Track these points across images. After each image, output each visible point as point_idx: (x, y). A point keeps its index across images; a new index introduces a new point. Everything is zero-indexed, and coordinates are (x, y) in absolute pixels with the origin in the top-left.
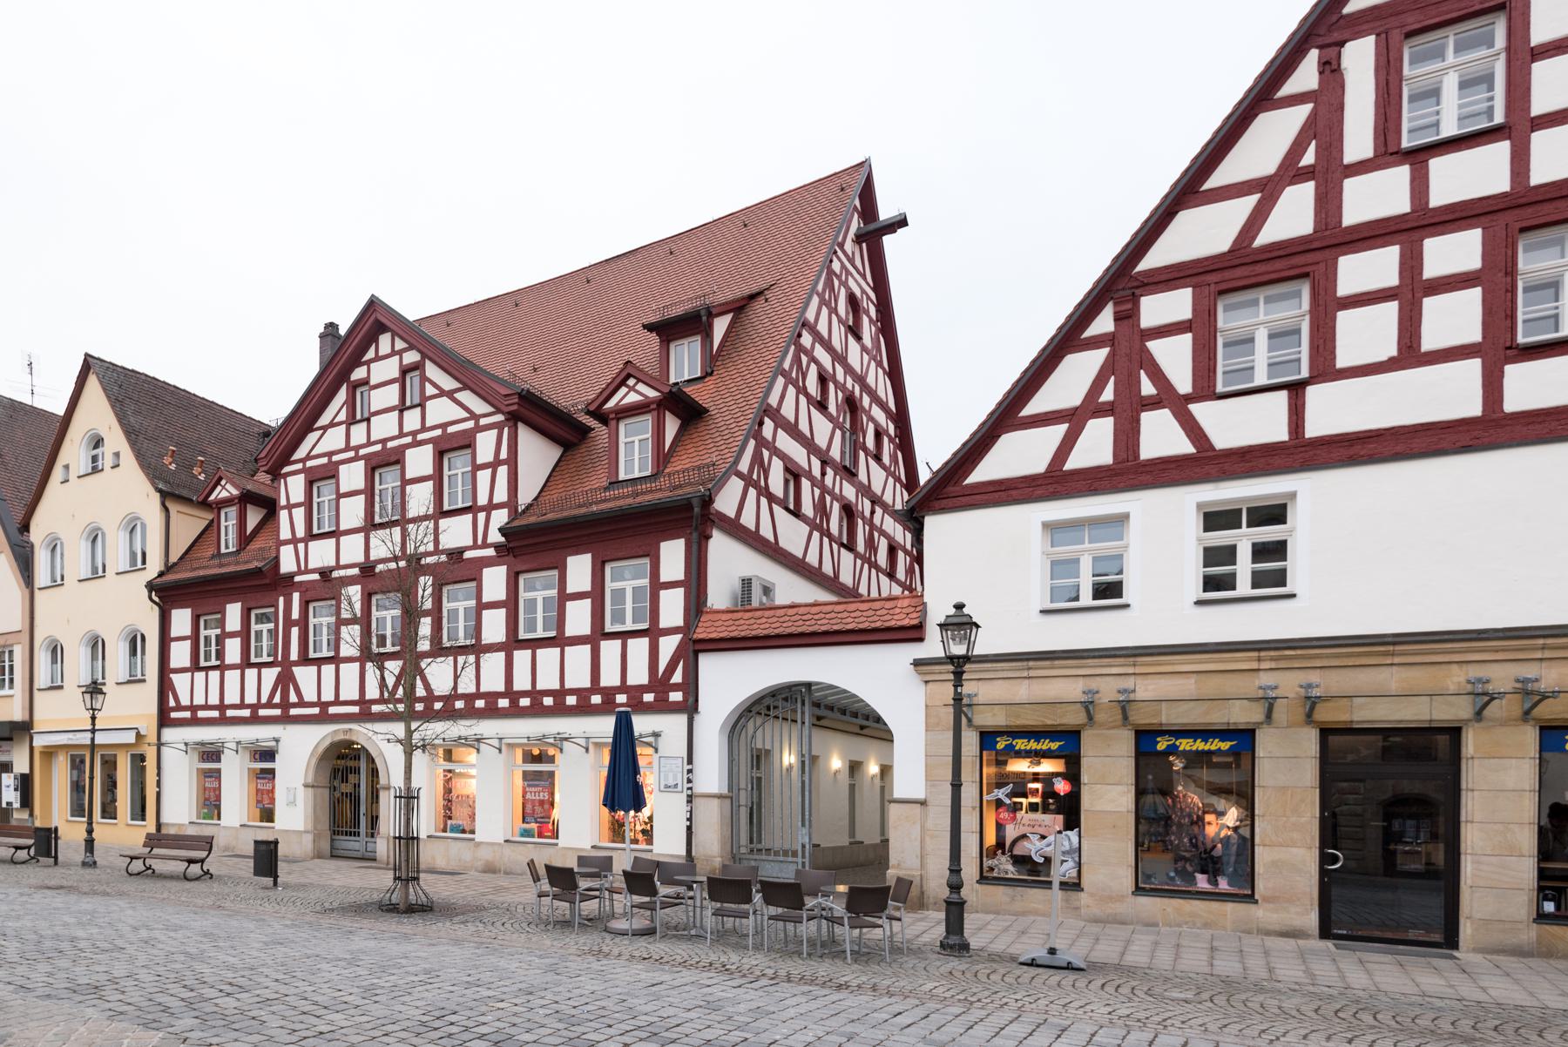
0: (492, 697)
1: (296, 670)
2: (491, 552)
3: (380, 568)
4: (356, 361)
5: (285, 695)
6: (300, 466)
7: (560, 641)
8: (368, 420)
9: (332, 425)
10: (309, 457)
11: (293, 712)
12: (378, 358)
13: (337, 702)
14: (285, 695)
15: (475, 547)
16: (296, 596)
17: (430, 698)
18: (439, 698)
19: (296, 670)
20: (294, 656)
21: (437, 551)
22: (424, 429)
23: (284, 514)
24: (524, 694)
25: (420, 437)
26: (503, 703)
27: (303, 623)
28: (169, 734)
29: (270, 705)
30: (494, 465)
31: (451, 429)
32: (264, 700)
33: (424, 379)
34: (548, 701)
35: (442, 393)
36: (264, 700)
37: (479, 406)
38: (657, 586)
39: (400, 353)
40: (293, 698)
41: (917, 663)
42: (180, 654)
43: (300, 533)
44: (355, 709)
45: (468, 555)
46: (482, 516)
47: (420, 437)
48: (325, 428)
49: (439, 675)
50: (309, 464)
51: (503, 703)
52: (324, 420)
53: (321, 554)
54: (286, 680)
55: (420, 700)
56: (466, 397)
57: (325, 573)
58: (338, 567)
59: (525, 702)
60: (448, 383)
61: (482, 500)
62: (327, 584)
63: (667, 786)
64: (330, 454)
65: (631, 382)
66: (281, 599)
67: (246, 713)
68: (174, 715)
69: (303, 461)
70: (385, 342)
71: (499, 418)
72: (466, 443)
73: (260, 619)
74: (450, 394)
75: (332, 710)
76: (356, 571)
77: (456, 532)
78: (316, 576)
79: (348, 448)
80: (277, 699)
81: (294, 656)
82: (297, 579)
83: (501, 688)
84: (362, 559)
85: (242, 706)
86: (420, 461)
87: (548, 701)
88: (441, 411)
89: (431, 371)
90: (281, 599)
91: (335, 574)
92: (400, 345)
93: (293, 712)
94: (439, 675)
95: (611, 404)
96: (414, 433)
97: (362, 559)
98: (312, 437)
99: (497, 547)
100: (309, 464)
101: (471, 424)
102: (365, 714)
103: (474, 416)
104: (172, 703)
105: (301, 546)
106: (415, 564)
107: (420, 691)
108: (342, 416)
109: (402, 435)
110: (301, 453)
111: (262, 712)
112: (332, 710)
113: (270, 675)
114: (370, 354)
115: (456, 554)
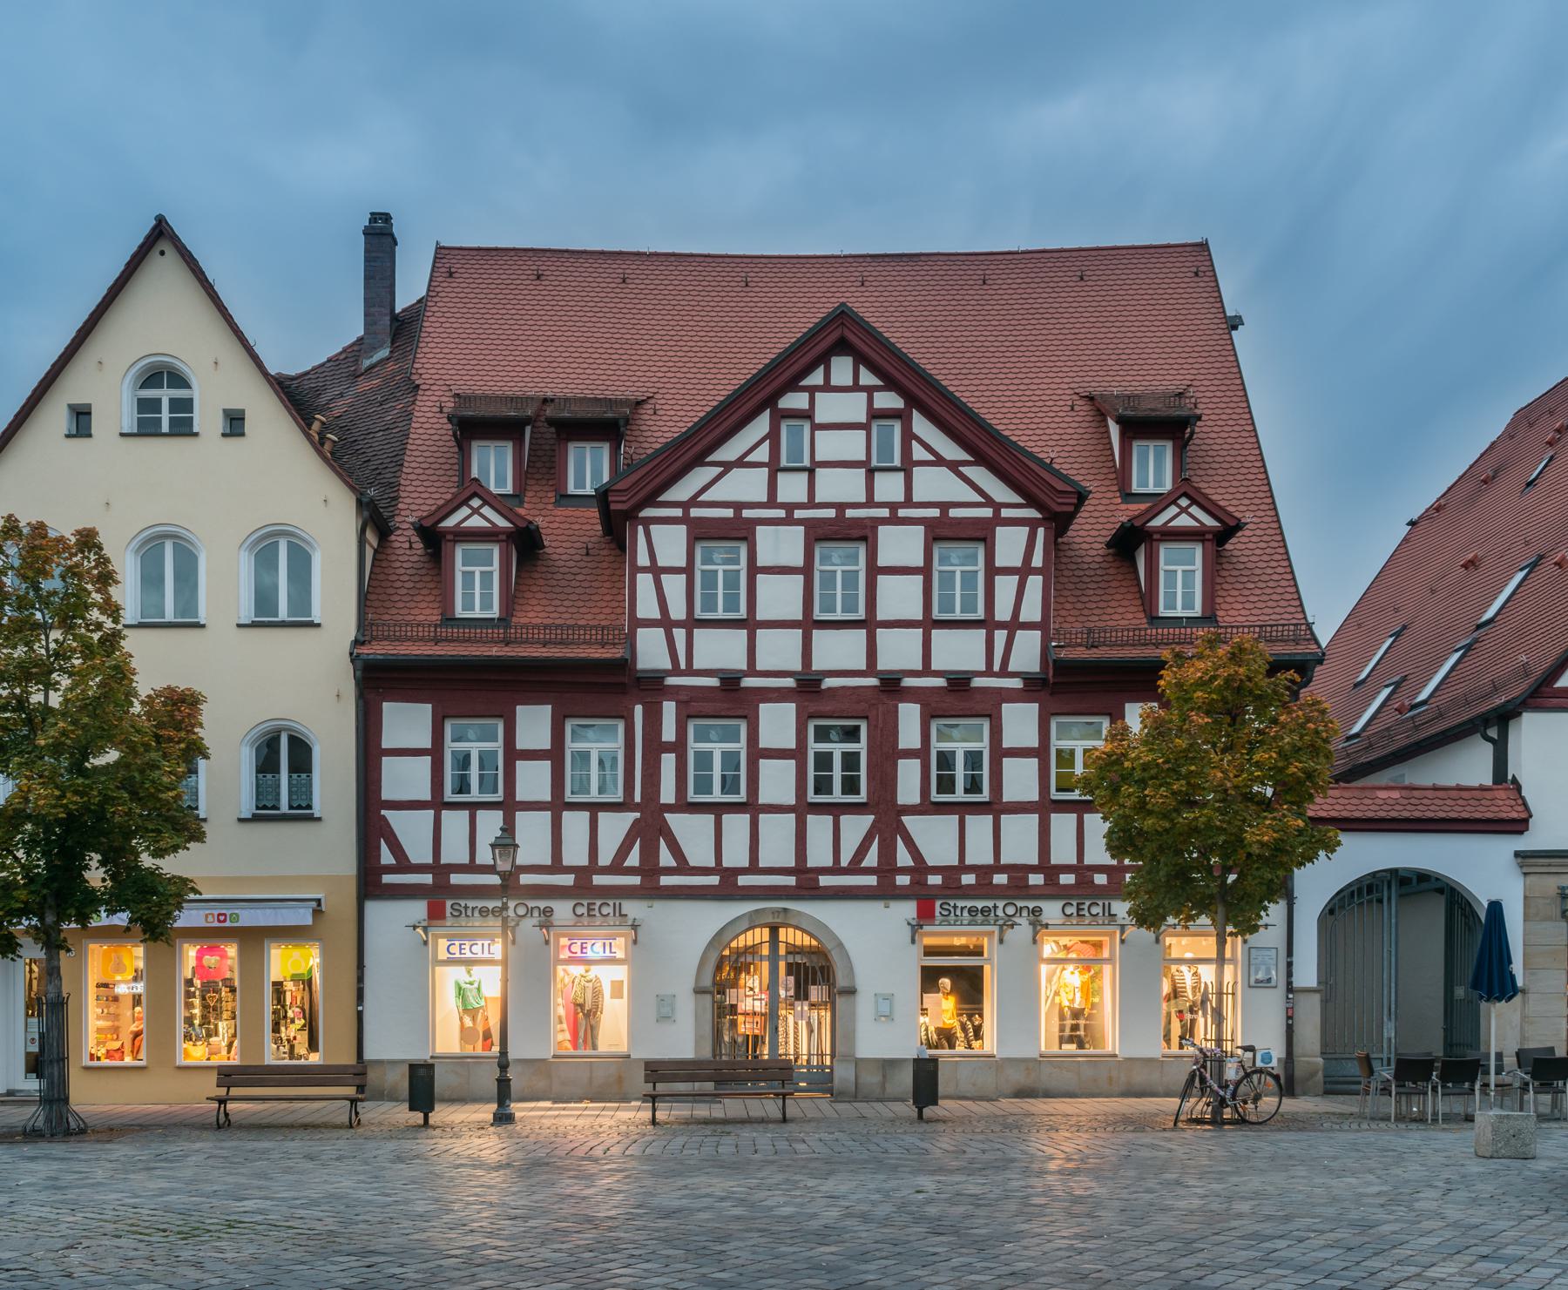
0: (1018, 872)
1: (670, 817)
2: (1016, 683)
3: (829, 682)
4: (793, 385)
5: (649, 853)
6: (678, 512)
7: (996, 808)
8: (811, 471)
9: (741, 463)
10: (693, 502)
11: (665, 880)
12: (827, 387)
13: (754, 868)
14: (649, 853)
15: (989, 672)
16: (669, 709)
17: (920, 868)
18: (936, 870)
19: (670, 817)
20: (668, 795)
21: (926, 671)
22: (909, 502)
23: (645, 582)
24: (1067, 869)
25: (798, 514)
26: (1036, 879)
27: (679, 747)
28: (373, 909)
29: (617, 867)
30: (1024, 571)
31: (953, 513)
32: (605, 859)
33: (908, 436)
34: (1101, 879)
35: (939, 461)
36: (605, 859)
37: (1000, 492)
38: (999, 753)
39: (870, 390)
40: (666, 858)
41: (1517, 854)
42: (405, 778)
43: (678, 611)
44: (791, 881)
45: (978, 682)
46: (1000, 636)
47: (902, 513)
48: (727, 466)
49: (935, 839)
50: (695, 512)
51: (1036, 879)
52: (730, 451)
53: (719, 651)
54: (651, 828)
55: (904, 871)
56: (979, 475)
57: (730, 681)
58: (752, 671)
59: (1067, 879)
60: (952, 451)
61: (1003, 612)
62: (733, 697)
63: (1257, 981)
64: (738, 506)
65: (476, 503)
66: (639, 709)
67: (568, 880)
68: (387, 879)
69: (686, 506)
70: (842, 369)
71: (1032, 513)
72: (982, 533)
73: (823, 734)
74: (954, 466)
75: (743, 880)
76: (789, 682)
77: (960, 651)
78: (713, 682)
79: (772, 502)
80: (633, 859)
81: (668, 795)
82: (671, 681)
83: (1035, 861)
84: (797, 666)
85: (557, 866)
86: (901, 545)
87: (1101, 879)
88: (934, 485)
89: (921, 425)
90: (639, 709)
91: (748, 682)
92: (867, 378)
93: (665, 880)
94: (935, 839)
95: (450, 522)
96: (790, 507)
97: (797, 666)
98: (698, 478)
99: (1028, 679)
100: (695, 512)
101: (987, 512)
102: (807, 883)
103: (989, 502)
104: (387, 857)
105: (1000, 636)
106: (892, 686)
107: (904, 858)
108: (762, 454)
109: (870, 502)
110: (681, 491)
111: (598, 880)
112: (743, 880)
113: (615, 827)
114: (817, 378)
115: (959, 683)
